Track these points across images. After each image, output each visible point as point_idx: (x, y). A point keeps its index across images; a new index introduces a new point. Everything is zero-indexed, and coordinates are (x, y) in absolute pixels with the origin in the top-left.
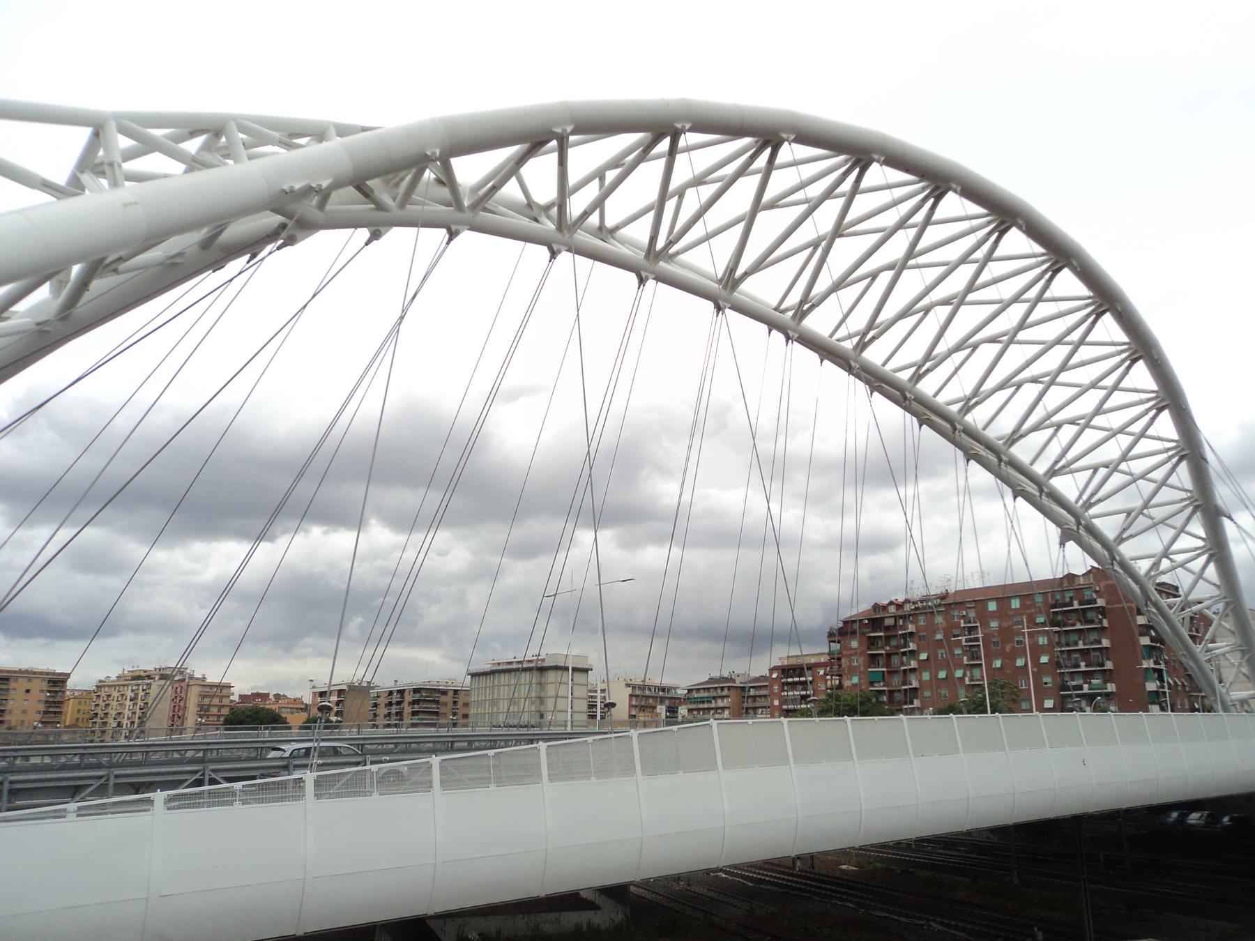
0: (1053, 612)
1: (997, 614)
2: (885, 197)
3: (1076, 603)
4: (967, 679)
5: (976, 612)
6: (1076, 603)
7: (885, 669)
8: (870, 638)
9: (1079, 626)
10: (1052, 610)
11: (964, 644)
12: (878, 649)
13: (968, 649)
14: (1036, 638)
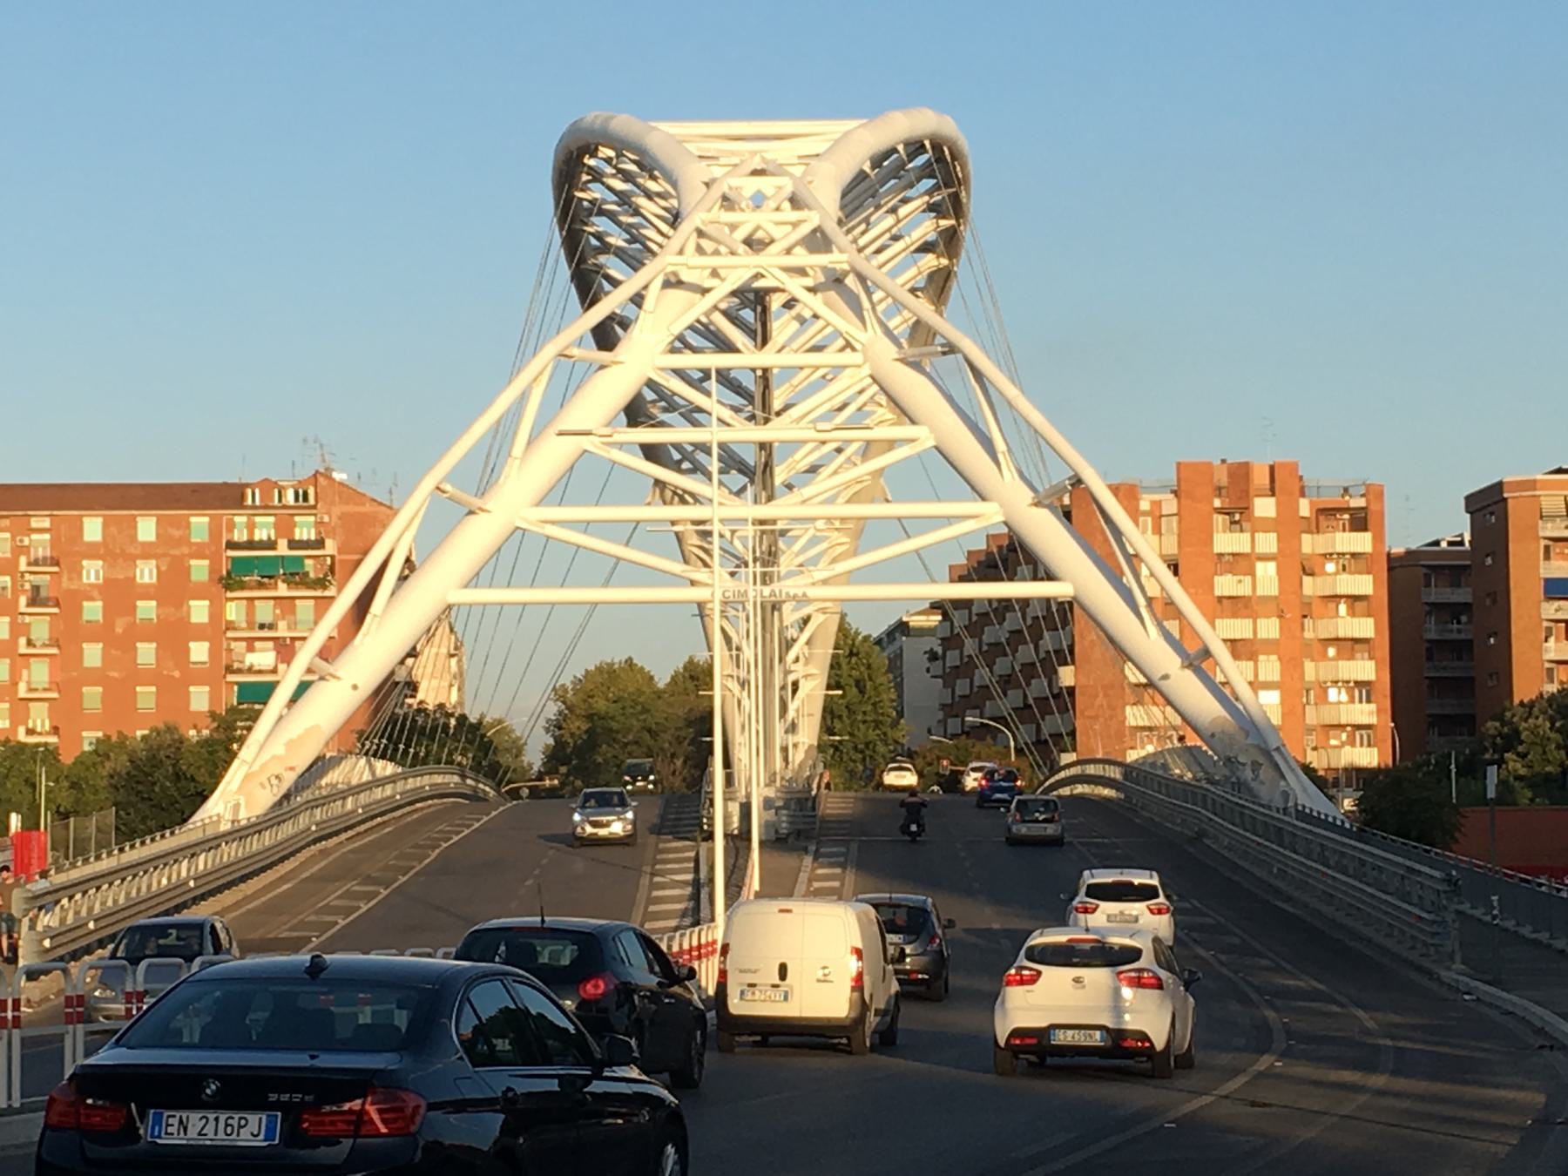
0: (227, 558)
1: (102, 552)
3: (282, 546)
5: (54, 543)
6: (282, 546)
14: (185, 608)
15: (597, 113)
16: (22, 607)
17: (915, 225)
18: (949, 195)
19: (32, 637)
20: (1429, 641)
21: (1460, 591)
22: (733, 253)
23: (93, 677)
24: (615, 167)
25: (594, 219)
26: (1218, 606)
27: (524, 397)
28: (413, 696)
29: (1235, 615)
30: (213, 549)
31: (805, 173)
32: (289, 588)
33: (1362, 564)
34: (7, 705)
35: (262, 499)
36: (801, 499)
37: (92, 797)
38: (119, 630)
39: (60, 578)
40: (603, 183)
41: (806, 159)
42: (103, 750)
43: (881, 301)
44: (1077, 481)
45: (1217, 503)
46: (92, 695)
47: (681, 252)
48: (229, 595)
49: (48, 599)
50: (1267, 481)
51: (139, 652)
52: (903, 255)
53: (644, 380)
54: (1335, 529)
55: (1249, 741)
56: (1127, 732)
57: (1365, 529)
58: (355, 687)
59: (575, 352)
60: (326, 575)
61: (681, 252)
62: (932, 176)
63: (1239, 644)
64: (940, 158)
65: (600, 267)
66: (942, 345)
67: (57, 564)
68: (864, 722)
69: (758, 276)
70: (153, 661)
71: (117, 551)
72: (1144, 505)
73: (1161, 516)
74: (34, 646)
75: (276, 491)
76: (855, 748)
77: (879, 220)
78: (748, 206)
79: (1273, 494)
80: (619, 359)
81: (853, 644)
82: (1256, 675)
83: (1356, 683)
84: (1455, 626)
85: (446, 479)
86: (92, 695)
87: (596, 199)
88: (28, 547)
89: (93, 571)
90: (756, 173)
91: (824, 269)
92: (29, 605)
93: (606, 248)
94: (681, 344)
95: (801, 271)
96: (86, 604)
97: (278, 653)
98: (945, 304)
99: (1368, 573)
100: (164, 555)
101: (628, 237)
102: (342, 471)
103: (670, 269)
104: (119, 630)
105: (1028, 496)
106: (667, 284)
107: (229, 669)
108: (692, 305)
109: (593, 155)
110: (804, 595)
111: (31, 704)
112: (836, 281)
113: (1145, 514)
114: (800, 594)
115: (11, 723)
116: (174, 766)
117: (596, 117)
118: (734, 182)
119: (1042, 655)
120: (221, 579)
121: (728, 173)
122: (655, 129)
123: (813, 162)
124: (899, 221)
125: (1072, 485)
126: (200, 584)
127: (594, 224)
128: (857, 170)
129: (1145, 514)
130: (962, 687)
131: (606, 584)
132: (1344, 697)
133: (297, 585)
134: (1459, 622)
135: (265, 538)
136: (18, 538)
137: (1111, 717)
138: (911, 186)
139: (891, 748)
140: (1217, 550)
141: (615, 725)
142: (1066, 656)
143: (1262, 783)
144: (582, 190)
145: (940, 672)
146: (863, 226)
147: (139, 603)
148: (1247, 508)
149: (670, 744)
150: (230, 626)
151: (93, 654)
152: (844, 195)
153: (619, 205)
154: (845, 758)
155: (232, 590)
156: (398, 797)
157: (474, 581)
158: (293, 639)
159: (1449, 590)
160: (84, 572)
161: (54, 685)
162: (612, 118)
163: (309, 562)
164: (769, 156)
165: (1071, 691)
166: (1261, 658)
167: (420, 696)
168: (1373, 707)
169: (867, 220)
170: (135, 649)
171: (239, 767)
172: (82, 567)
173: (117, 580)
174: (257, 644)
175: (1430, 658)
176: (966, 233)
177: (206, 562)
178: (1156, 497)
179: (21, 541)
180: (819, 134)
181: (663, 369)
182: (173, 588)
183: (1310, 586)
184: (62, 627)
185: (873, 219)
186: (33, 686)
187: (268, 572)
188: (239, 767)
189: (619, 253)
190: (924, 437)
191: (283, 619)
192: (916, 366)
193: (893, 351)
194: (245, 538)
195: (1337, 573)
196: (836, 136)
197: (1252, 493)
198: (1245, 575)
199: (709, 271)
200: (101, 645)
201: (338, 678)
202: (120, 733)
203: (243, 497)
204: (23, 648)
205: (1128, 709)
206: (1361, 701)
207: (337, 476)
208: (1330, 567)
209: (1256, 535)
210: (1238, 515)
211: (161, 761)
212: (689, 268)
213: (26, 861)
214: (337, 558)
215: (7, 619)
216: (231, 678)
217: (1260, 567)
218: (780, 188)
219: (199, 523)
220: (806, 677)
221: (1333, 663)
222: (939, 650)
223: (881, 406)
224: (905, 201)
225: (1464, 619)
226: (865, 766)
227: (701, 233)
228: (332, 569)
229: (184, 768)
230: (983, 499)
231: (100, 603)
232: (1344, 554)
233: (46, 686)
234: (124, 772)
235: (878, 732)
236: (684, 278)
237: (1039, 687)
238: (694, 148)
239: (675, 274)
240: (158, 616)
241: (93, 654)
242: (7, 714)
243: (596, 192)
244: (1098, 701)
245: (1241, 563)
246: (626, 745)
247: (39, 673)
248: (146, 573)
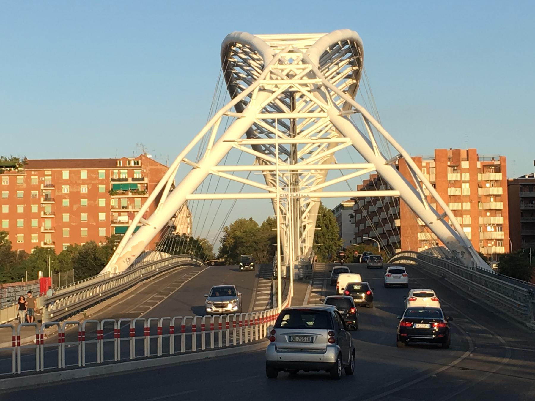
1: (69, 182)
5: (53, 180)
10: (112, 183)
14: (97, 202)
15: (235, 32)
16: (42, 201)
17: (345, 69)
18: (356, 59)
19: (46, 212)
20: (522, 210)
21: (533, 192)
22: (282, 79)
23: (66, 225)
24: (242, 50)
25: (235, 68)
26: (449, 198)
27: (211, 129)
28: (175, 231)
29: (455, 202)
30: (106, 181)
31: (307, 52)
33: (499, 184)
34: (37, 235)
35: (123, 165)
36: (306, 163)
37: (66, 266)
38: (75, 209)
40: (238, 56)
41: (307, 47)
42: (70, 250)
43: (333, 95)
44: (401, 156)
45: (449, 163)
46: (66, 231)
47: (265, 79)
48: (112, 197)
49: (51, 199)
50: (466, 156)
51: (82, 216)
52: (341, 79)
53: (252, 123)
54: (489, 172)
55: (460, 245)
56: (418, 242)
57: (500, 172)
58: (155, 228)
59: (229, 113)
60: (145, 190)
61: (265, 79)
62: (350, 52)
63: (456, 211)
64: (353, 46)
65: (237, 84)
66: (354, 110)
67: (54, 187)
68: (328, 239)
69: (291, 87)
70: (86, 219)
71: (74, 182)
72: (424, 164)
73: (430, 168)
74: (46, 215)
75: (128, 161)
76: (326, 248)
77: (333, 67)
78: (287, 63)
79: (468, 160)
80: (244, 115)
81: (325, 213)
82: (463, 222)
83: (498, 225)
84: (531, 205)
85: (185, 157)
86: (66, 231)
87: (236, 61)
88: (44, 181)
89: (66, 189)
90: (290, 52)
91: (314, 84)
92: (44, 201)
93: (239, 78)
94: (265, 110)
95: (306, 85)
96: (63, 200)
97: (129, 216)
98: (355, 96)
99: (501, 187)
101: (246, 74)
102: (150, 154)
103: (261, 85)
104: (75, 209)
105: (384, 161)
106: (260, 90)
107: (113, 222)
108: (268, 97)
109: (235, 46)
110: (308, 196)
111: (46, 234)
112: (318, 88)
113: (424, 167)
114: (306, 195)
115: (39, 241)
116: (94, 255)
117: (235, 33)
118: (283, 55)
119: (389, 216)
120: (109, 192)
121: (280, 52)
122: (255, 37)
123: (310, 48)
124: (339, 68)
125: (399, 157)
126: (102, 193)
127: (235, 70)
128: (324, 50)
129: (424, 167)
130: (362, 227)
131: (240, 193)
132: (493, 229)
133: (135, 193)
134: (532, 204)
135: (124, 177)
136: (41, 178)
137: (413, 237)
138: (343, 55)
139: (338, 248)
140: (448, 179)
141: (243, 241)
142: (397, 216)
143: (465, 259)
144: (231, 58)
145: (354, 222)
146: (327, 70)
147: (82, 200)
148: (459, 165)
149: (262, 246)
150: (113, 207)
151: (66, 217)
152: (320, 59)
153: (243, 63)
154: (322, 251)
155: (113, 195)
156: (170, 265)
157: (195, 192)
158: (133, 211)
159: (529, 193)
160: (63, 190)
161: (53, 228)
162: (242, 33)
163: (139, 185)
164: (294, 46)
165: (399, 228)
166: (464, 216)
167: (177, 231)
168: (503, 233)
169: (328, 68)
170: (80, 215)
171: (116, 255)
172: (62, 188)
173: (74, 192)
174: (122, 214)
175: (522, 216)
176: (362, 71)
177: (104, 186)
178: (428, 161)
179: (42, 179)
180: (312, 38)
181: (258, 119)
182: (93, 195)
183: (481, 191)
184: (56, 208)
185: (330, 67)
186: (46, 228)
187: (125, 189)
188: (116, 255)
189: (244, 79)
190: (348, 142)
191: (130, 205)
192: (345, 117)
193: (337, 112)
194: (117, 177)
195: (490, 187)
196: (317, 39)
197: (461, 160)
198: (459, 188)
199: (274, 85)
200: (69, 214)
201: (149, 225)
202: (75, 244)
203: (116, 163)
204: (42, 216)
205: (419, 234)
206: (499, 231)
207: (149, 156)
208: (488, 185)
209: (463, 175)
210: (456, 167)
211: (89, 254)
212: (268, 84)
213: (44, 287)
214: (149, 184)
215: (37, 206)
216: (113, 225)
217: (464, 185)
218: (298, 57)
219: (102, 172)
220: (308, 223)
221: (489, 218)
222: (354, 214)
223: (333, 131)
224: (341, 61)
225: (533, 202)
226: (329, 254)
227: (271, 72)
228: (147, 188)
229: (97, 256)
230: (369, 162)
231: (68, 200)
232: (492, 180)
233: (51, 228)
234: (77, 257)
235: (333, 242)
236: (266, 88)
237: (388, 227)
238: (269, 43)
239: (263, 86)
240: (88, 204)
241: (66, 217)
242: (37, 238)
243: (236, 59)
244: (408, 232)
245: (457, 184)
246: (247, 247)
247: (48, 224)
248: (84, 190)
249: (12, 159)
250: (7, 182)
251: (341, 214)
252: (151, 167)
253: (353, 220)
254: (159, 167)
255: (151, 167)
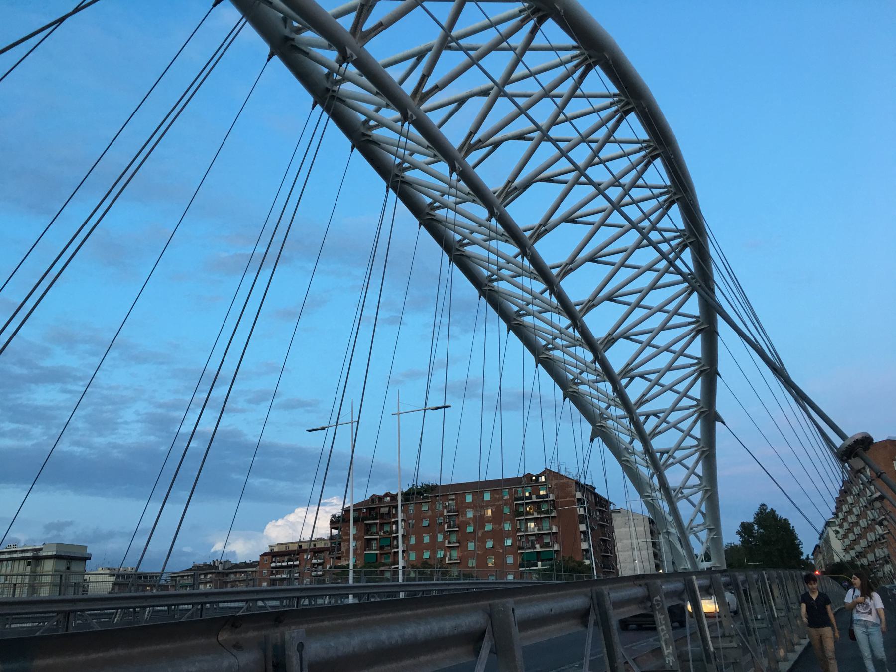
0: (516, 504)
1: (472, 505)
2: (551, 58)
3: (534, 497)
4: (447, 559)
5: (457, 503)
6: (534, 497)
7: (378, 552)
8: (367, 524)
9: (535, 515)
11: (446, 529)
12: (372, 534)
13: (448, 533)
14: (502, 525)
32: (538, 514)
39: (459, 518)
48: (517, 518)
67: (458, 511)
89: (470, 515)
92: (448, 528)
100: (494, 505)
107: (520, 548)
130: (847, 542)
151: (471, 546)
158: (541, 534)
179: (445, 504)
182: (498, 518)
184: (460, 535)
204: (446, 545)
233: (456, 558)
240: (493, 528)
249: (422, 486)
250: (413, 510)
251: (828, 531)
252: (556, 482)
253: (839, 536)
254: (565, 480)
255: (556, 482)
